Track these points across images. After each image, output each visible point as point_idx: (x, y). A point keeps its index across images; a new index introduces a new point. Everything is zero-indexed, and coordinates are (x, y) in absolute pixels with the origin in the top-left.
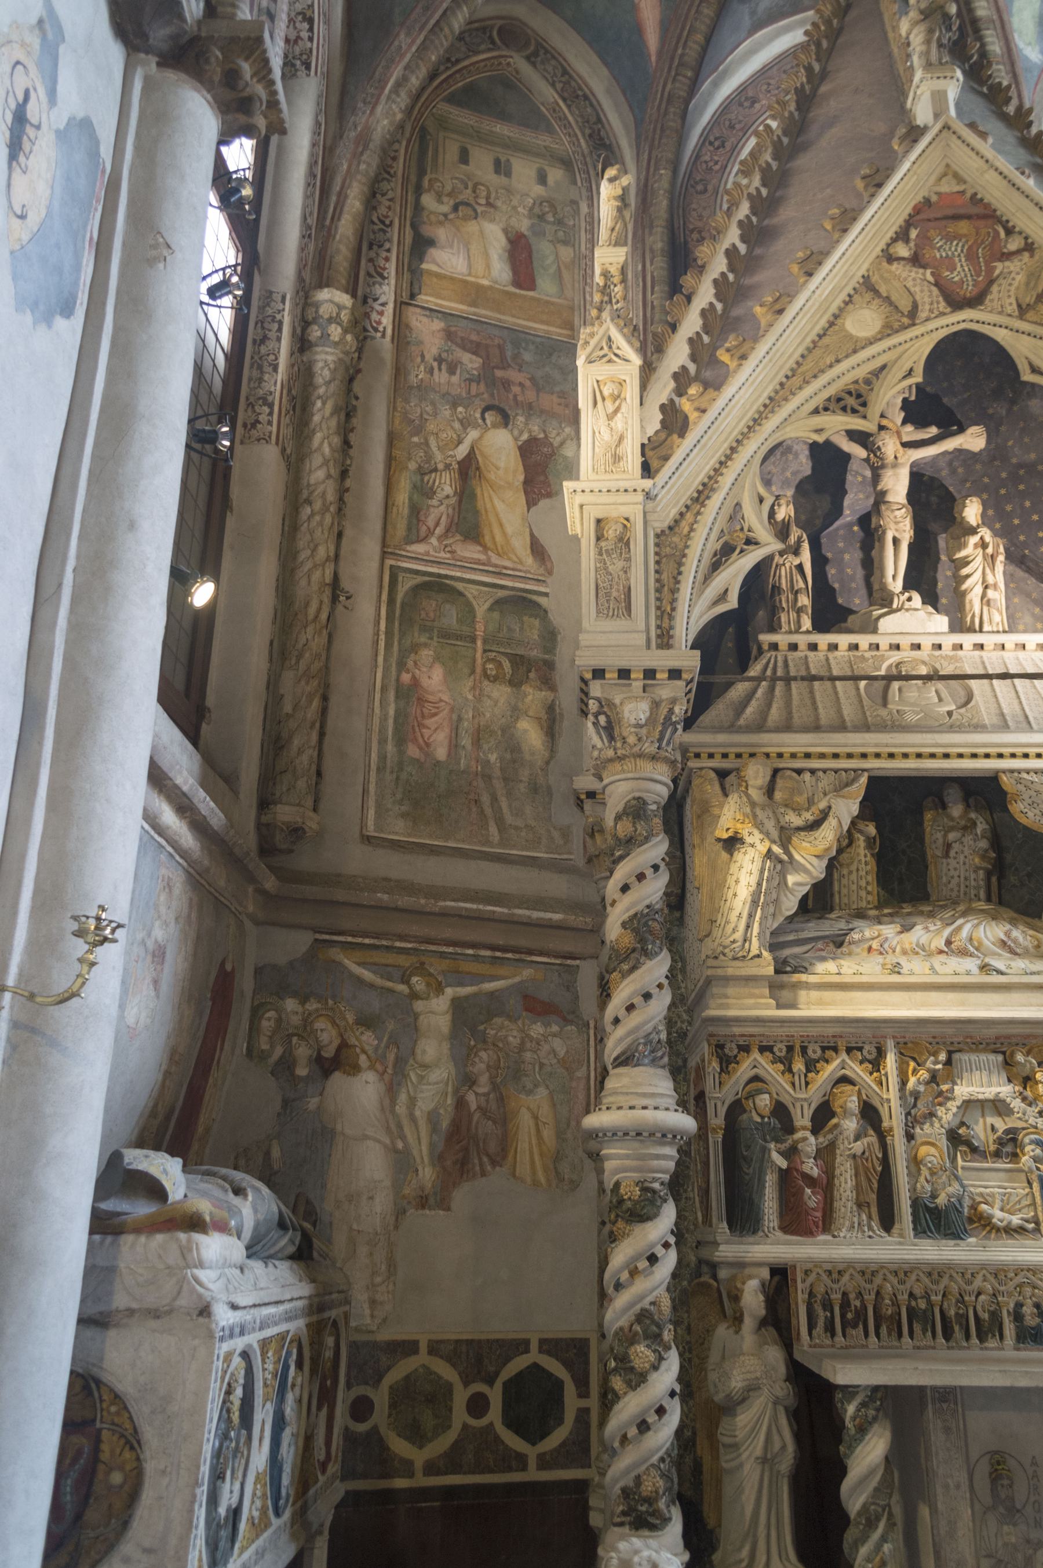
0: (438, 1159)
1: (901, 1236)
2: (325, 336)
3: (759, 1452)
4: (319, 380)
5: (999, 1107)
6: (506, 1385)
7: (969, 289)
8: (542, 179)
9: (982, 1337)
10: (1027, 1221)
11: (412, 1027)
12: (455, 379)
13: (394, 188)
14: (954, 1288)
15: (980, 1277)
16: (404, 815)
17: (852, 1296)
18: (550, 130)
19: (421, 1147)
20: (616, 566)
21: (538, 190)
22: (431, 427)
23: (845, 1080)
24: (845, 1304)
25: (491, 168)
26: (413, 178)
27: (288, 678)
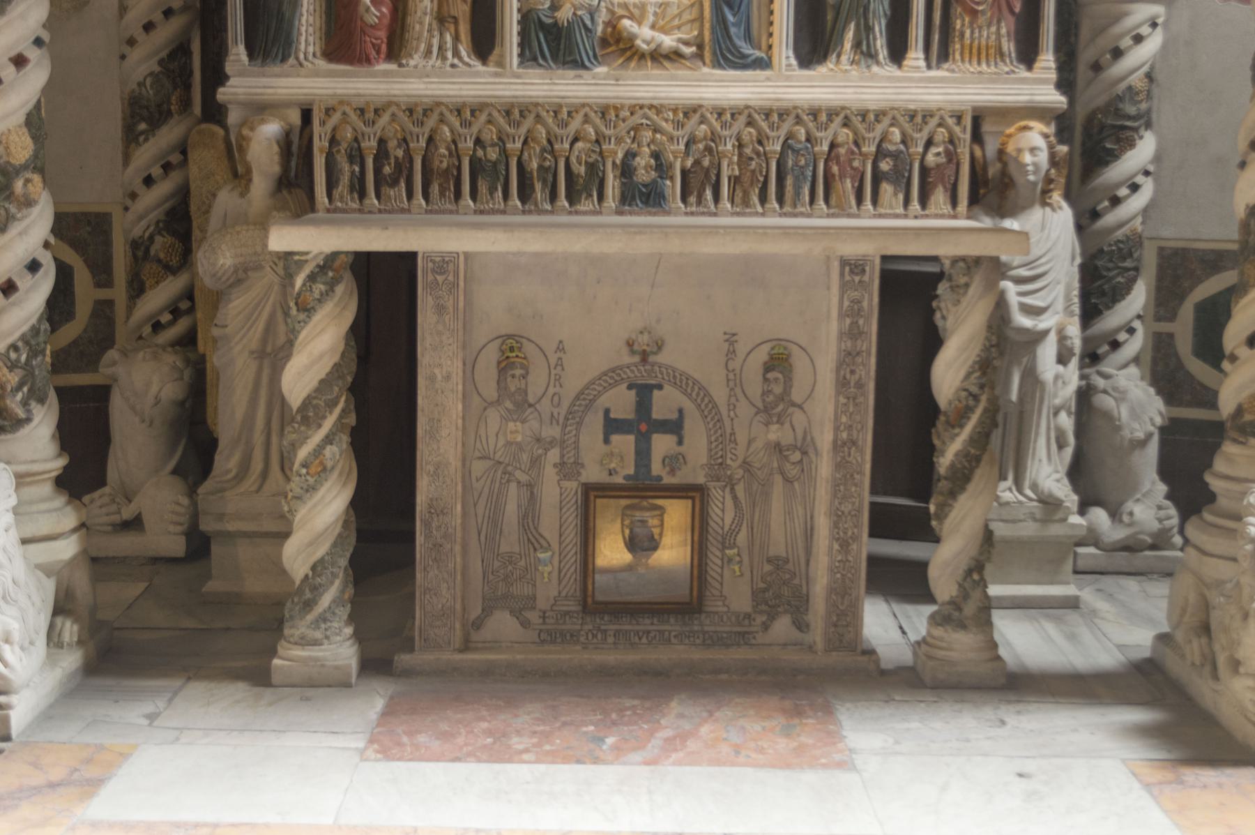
1: (500, 64)
3: (254, 345)
9: (572, 198)
10: (687, 43)
14: (542, 132)
15: (579, 118)
17: (392, 144)
24: (382, 153)
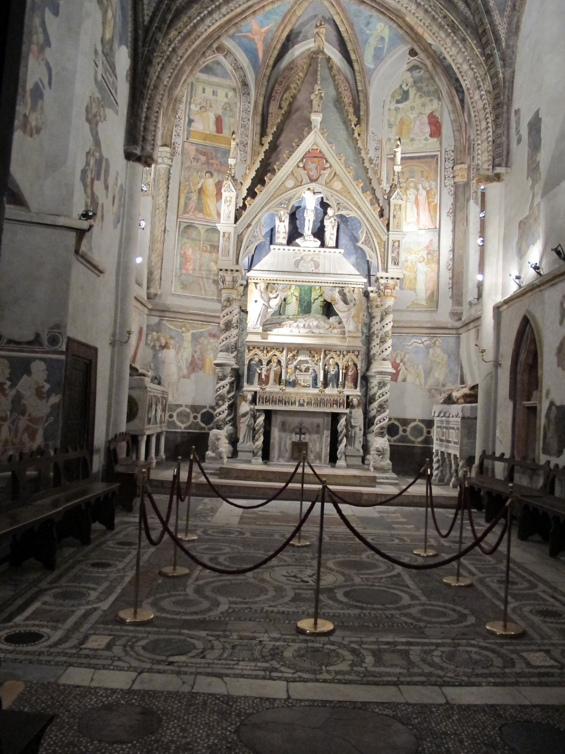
5: (306, 362)
7: (315, 177)
8: (227, 96)
11: (182, 339)
12: (198, 164)
18: (230, 79)
20: (227, 244)
21: (226, 100)
22: (191, 179)
23: (275, 355)
26: (189, 100)
27: (153, 256)
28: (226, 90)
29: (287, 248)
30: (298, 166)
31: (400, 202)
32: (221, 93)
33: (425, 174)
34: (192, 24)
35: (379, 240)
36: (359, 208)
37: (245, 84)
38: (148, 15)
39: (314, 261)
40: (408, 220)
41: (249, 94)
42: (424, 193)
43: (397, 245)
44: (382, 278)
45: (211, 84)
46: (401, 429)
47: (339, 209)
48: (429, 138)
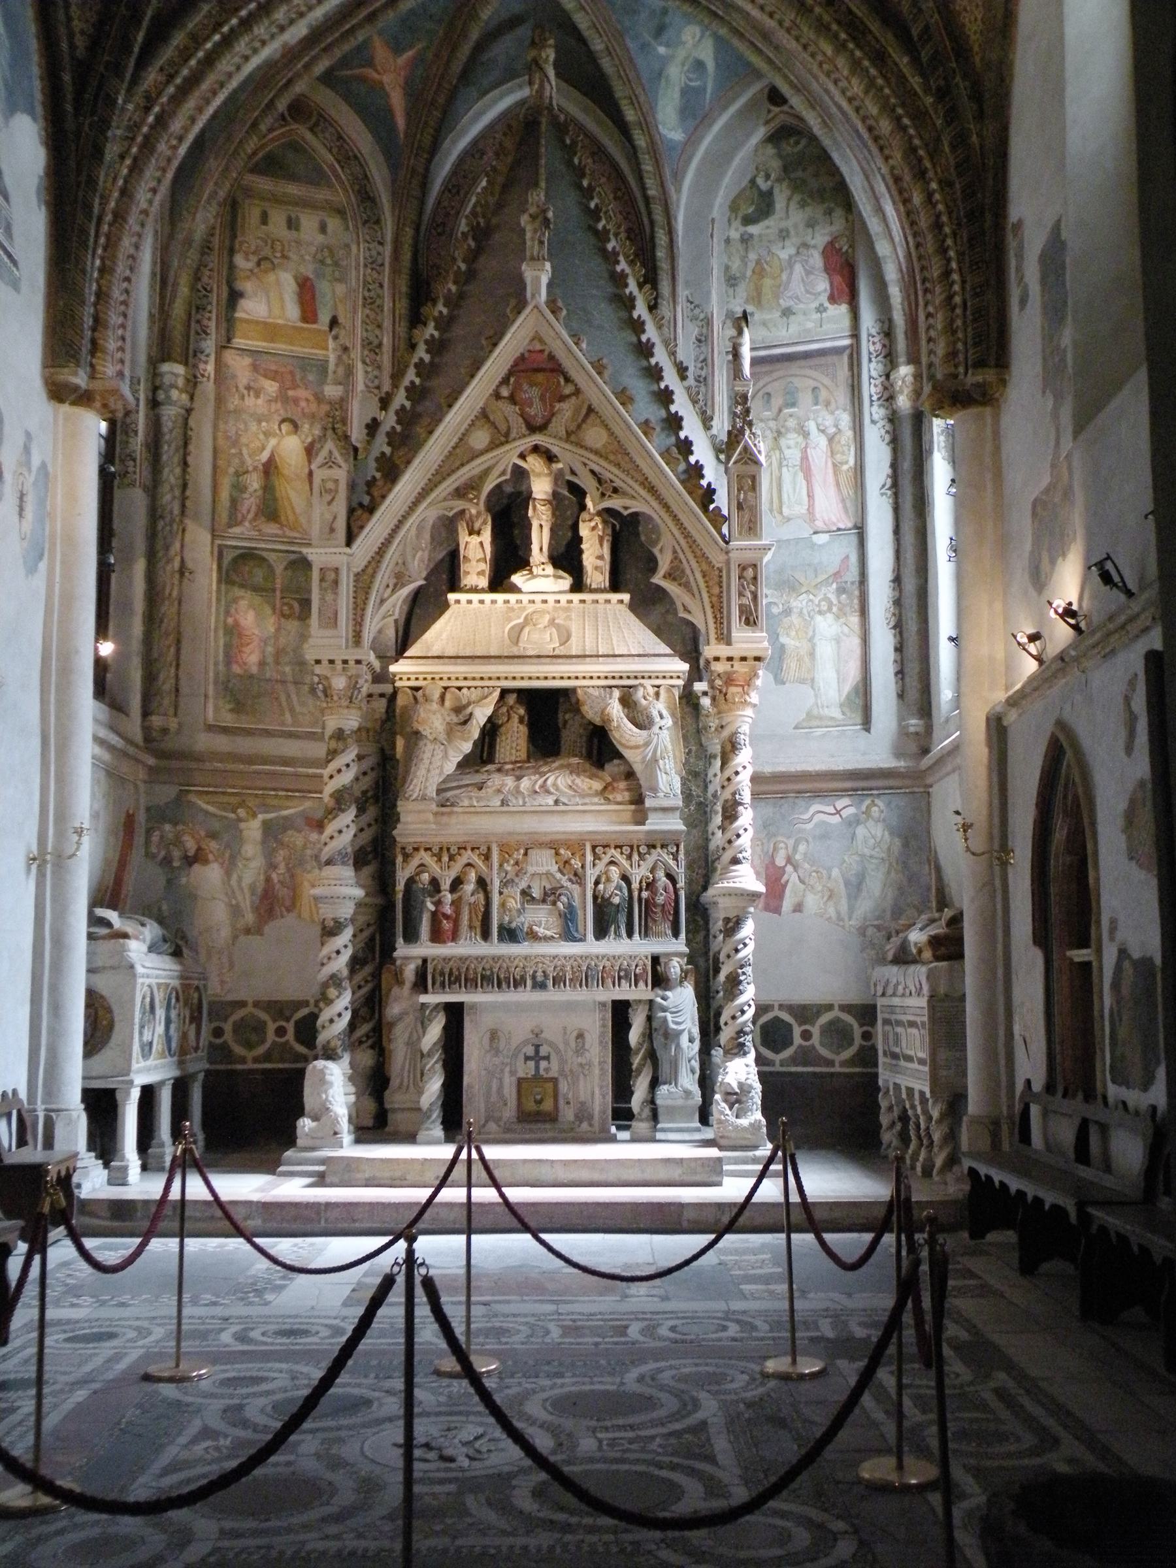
0: (256, 909)
2: (168, 397)
4: (165, 430)
5: (548, 874)
6: (296, 1023)
7: (539, 421)
8: (323, 228)
11: (239, 838)
12: (260, 401)
13: (213, 260)
16: (231, 710)
18: (330, 186)
19: (246, 902)
20: (329, 597)
21: (320, 238)
22: (244, 440)
24: (451, 974)
25: (284, 224)
26: (227, 243)
28: (323, 215)
29: (488, 597)
30: (497, 396)
31: (751, 469)
32: (309, 222)
33: (823, 394)
34: (201, 54)
35: (705, 567)
36: (652, 490)
37: (366, 197)
38: (82, 32)
39: (558, 627)
40: (786, 511)
41: (378, 222)
42: (823, 441)
43: (750, 573)
44: (717, 659)
45: (278, 200)
46: (797, 1031)
47: (603, 495)
48: (827, 304)
